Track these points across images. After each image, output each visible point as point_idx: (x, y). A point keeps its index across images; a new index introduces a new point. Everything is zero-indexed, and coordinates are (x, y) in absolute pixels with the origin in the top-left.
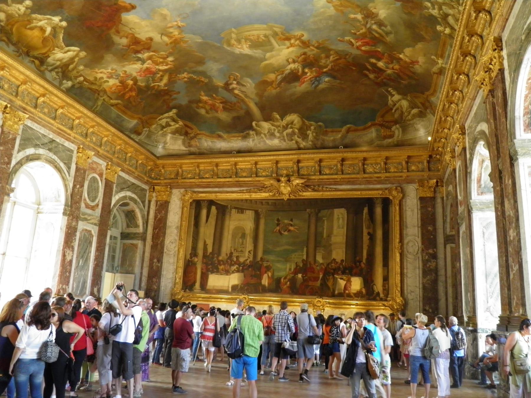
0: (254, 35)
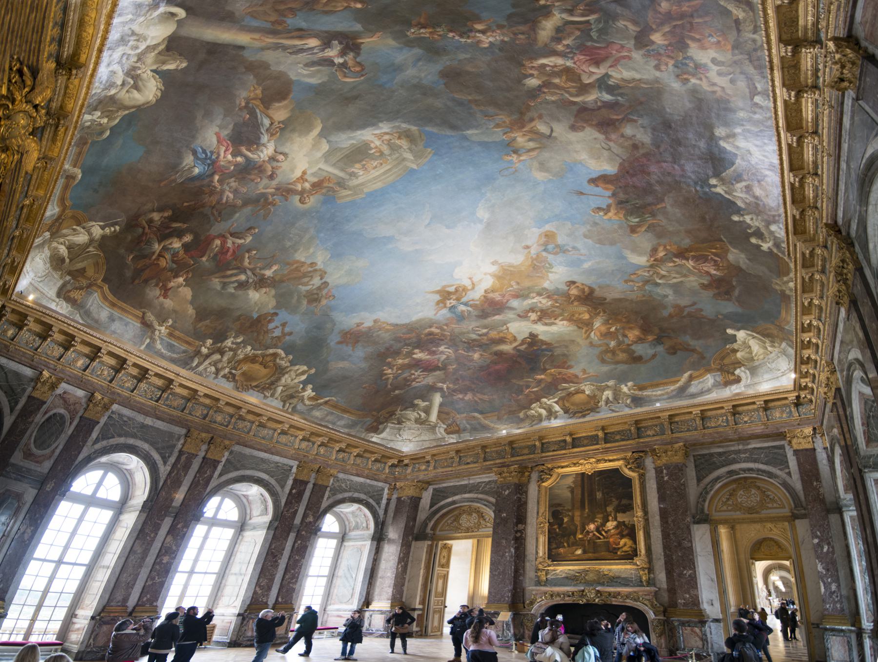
0: (376, 167)
